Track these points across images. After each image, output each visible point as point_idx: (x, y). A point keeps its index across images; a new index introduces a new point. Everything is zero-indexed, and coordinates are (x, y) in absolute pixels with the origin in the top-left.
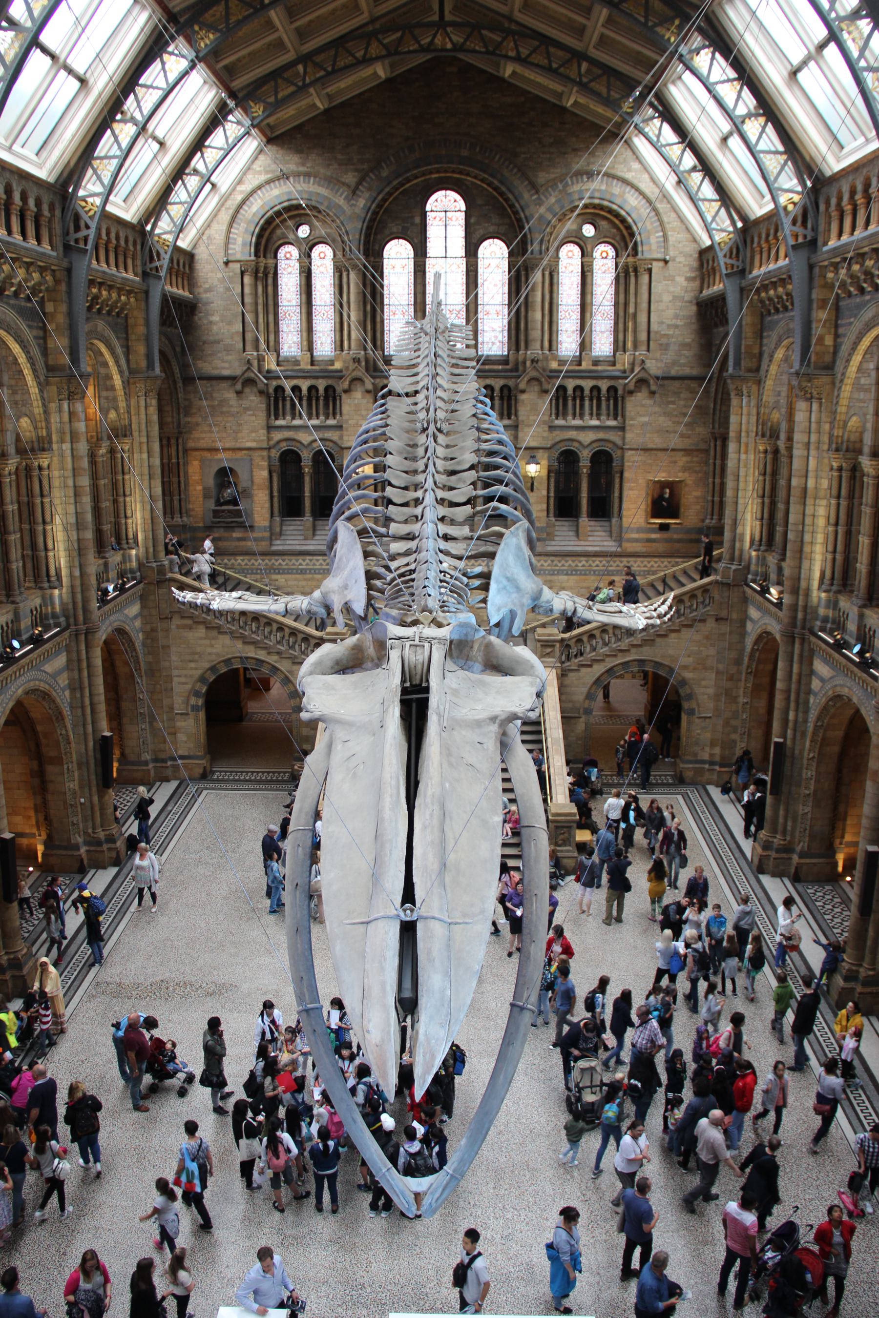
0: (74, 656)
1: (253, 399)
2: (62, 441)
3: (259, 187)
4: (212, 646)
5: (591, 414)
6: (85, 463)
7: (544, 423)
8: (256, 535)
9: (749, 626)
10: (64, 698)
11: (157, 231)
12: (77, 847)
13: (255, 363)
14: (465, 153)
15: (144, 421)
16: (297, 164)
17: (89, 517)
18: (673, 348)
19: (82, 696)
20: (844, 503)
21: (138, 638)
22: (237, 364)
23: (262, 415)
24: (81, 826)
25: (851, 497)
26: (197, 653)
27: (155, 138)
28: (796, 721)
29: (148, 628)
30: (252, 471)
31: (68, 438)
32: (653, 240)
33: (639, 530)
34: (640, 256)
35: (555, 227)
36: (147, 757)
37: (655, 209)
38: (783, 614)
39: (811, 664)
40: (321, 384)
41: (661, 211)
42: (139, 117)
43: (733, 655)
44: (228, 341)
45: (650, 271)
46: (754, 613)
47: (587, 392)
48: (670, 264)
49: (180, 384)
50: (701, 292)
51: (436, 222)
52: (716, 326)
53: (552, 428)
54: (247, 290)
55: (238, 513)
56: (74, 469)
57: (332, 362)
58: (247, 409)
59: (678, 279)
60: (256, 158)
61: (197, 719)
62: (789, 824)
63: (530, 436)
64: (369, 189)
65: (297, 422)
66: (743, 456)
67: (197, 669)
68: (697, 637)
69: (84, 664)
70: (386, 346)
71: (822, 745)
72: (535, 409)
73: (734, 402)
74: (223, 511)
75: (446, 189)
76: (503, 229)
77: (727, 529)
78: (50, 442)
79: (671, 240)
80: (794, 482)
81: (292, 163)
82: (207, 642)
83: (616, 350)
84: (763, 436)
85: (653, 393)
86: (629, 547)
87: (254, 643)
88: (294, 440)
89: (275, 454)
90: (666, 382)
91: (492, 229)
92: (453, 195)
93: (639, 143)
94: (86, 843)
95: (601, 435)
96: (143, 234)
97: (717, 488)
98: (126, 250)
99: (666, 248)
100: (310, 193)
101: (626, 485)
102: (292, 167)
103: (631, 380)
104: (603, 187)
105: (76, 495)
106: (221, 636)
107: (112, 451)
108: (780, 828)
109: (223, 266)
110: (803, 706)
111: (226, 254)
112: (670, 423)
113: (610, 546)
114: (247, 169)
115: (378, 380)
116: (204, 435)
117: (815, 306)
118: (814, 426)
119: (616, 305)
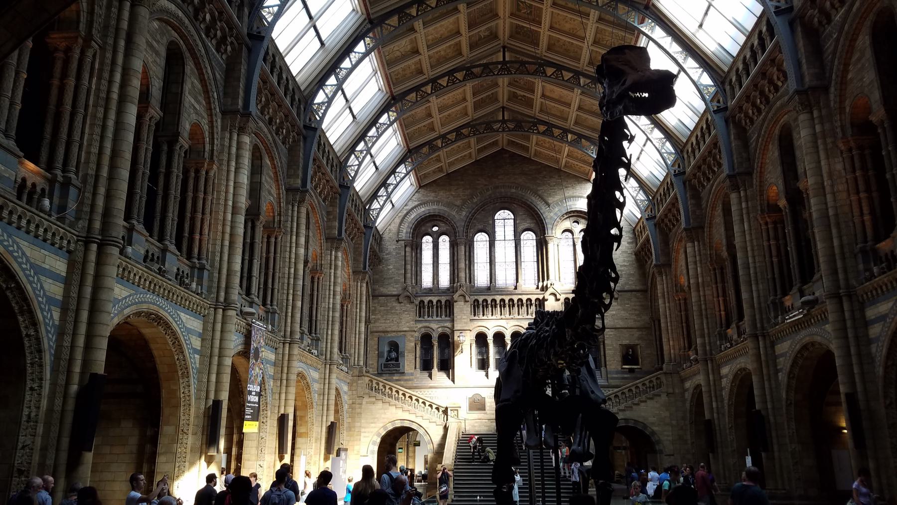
2: (330, 269)
3: (415, 207)
4: (385, 413)
8: (405, 378)
13: (410, 288)
14: (514, 191)
16: (433, 197)
20: (720, 285)
23: (413, 314)
28: (717, 407)
29: (351, 402)
31: (333, 267)
33: (617, 372)
40: (443, 299)
44: (397, 278)
49: (371, 298)
51: (500, 224)
54: (407, 254)
57: (448, 289)
58: (405, 311)
66: (667, 305)
69: (327, 381)
70: (476, 282)
73: (658, 279)
74: (389, 364)
76: (532, 226)
81: (431, 196)
82: (383, 411)
88: (428, 327)
89: (417, 334)
90: (622, 293)
91: (526, 225)
92: (507, 212)
101: (607, 348)
102: (432, 198)
106: (391, 408)
109: (396, 243)
110: (719, 398)
112: (628, 314)
115: (472, 297)
116: (381, 325)
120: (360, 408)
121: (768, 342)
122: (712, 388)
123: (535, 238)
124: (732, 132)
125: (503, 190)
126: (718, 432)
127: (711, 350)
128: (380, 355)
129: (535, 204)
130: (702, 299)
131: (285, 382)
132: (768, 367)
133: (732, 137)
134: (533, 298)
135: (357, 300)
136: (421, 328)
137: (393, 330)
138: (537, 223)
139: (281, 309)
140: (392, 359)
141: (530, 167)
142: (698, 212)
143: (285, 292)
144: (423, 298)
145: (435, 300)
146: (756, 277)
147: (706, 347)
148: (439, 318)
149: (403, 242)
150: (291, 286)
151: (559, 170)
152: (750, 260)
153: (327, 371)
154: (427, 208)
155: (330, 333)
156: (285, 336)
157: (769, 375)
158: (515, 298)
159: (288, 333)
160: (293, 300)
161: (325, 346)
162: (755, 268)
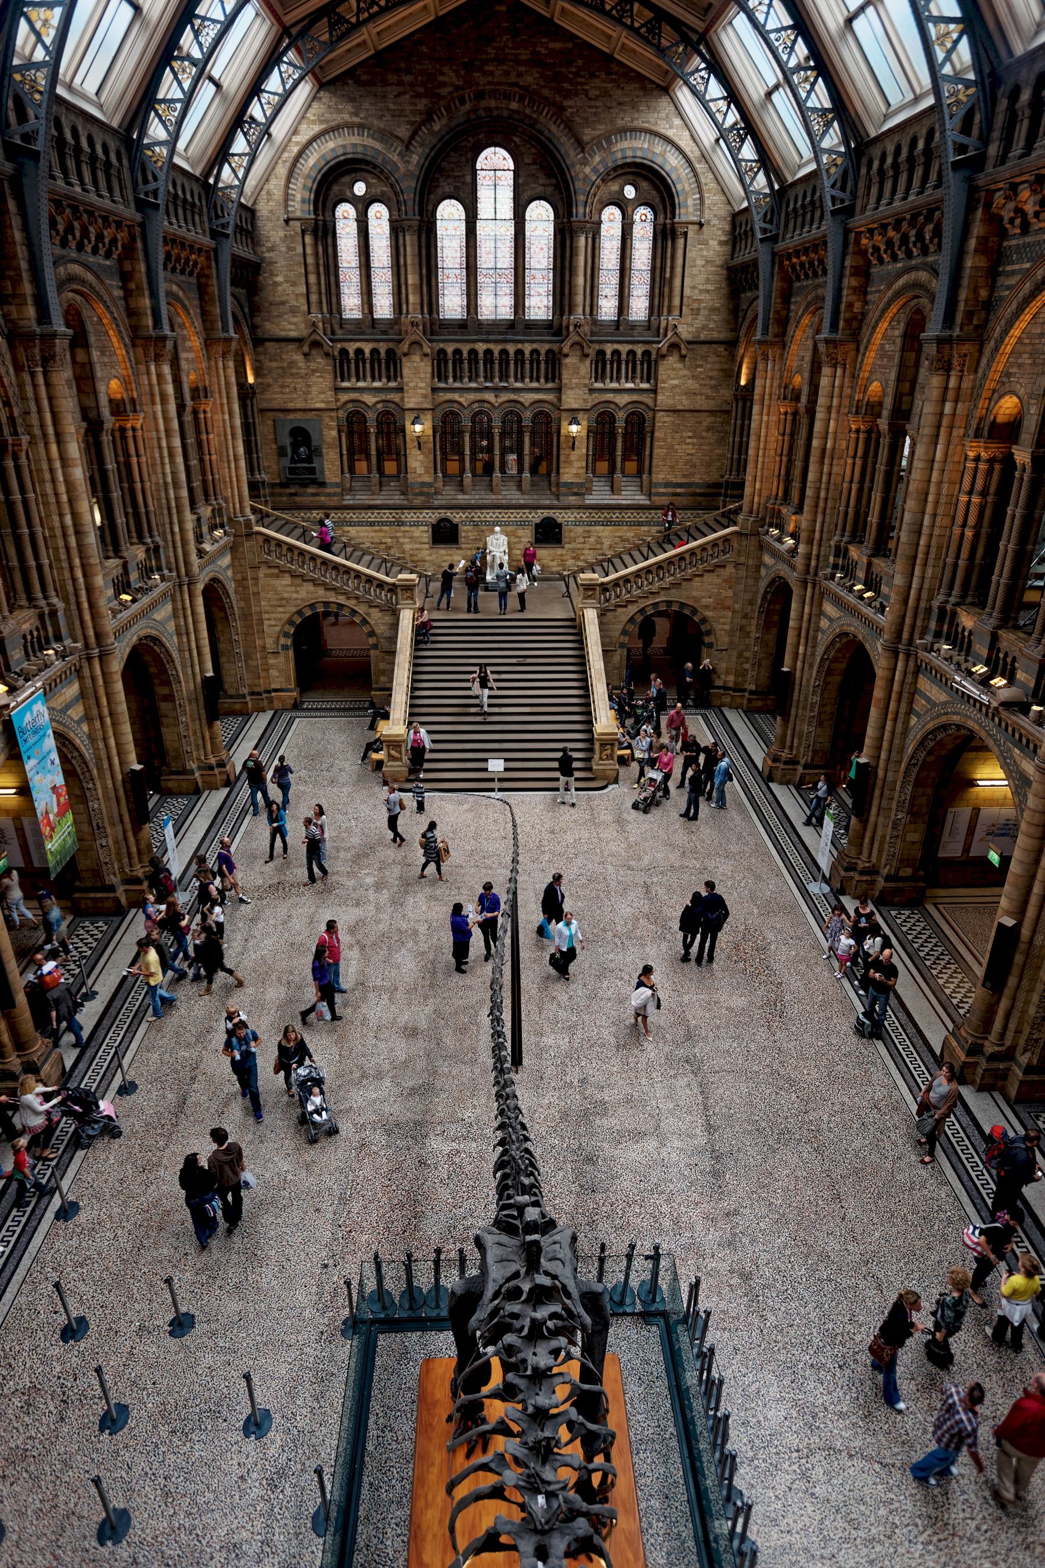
0: (180, 607)
1: (320, 362)
2: (153, 403)
4: (297, 592)
5: (627, 378)
6: (175, 425)
7: (585, 385)
8: (328, 490)
9: (763, 572)
10: (172, 643)
11: (220, 185)
12: (192, 772)
13: (320, 325)
14: (514, 105)
15: (223, 383)
16: (351, 114)
17: (183, 476)
18: (704, 312)
19: (189, 641)
20: (859, 462)
21: (231, 587)
22: (303, 326)
23: (329, 377)
24: (195, 754)
25: (865, 457)
26: (282, 599)
27: (211, 79)
28: (805, 654)
29: (239, 577)
30: (321, 431)
31: (158, 399)
32: (690, 202)
33: (667, 485)
34: (677, 220)
35: (598, 187)
36: (246, 691)
37: (693, 170)
38: (799, 561)
39: (821, 605)
40: (383, 348)
41: (699, 171)
42: (196, 54)
43: (748, 596)
44: (294, 303)
45: (686, 234)
46: (768, 559)
47: (624, 356)
48: (705, 228)
50: (732, 258)
52: (744, 291)
53: (592, 391)
54: (309, 250)
55: (312, 471)
56: (166, 431)
58: (314, 371)
59: (711, 242)
60: (310, 106)
61: (287, 658)
62: (796, 740)
63: (572, 399)
64: (422, 145)
65: (361, 384)
66: (765, 418)
67: (284, 614)
68: (719, 581)
69: (189, 612)
71: (827, 675)
72: (576, 371)
73: (760, 366)
75: (495, 145)
76: (549, 190)
77: (747, 484)
78: (141, 405)
79: (707, 202)
80: (815, 443)
82: (293, 589)
83: (651, 314)
84: (785, 398)
85: (683, 357)
86: (659, 501)
87: (335, 589)
89: (342, 414)
91: (539, 190)
92: (502, 152)
93: (684, 96)
94: (200, 768)
95: (635, 397)
96: (206, 186)
97: (736, 446)
98: (193, 205)
99: (702, 211)
100: (365, 146)
101: (656, 444)
102: (346, 117)
103: (663, 345)
104: (646, 146)
105: (171, 455)
107: (195, 412)
108: (788, 743)
110: (811, 641)
111: (287, 212)
113: (642, 499)
114: (302, 117)
117: (847, 272)
118: (836, 390)
119: (653, 270)
120: (257, 584)
121: (911, 664)
122: (804, 625)
123: (552, 217)
124: (977, 229)
125: (493, 104)
126: (797, 687)
127: (817, 567)
128: (281, 452)
129: (555, 141)
130: (825, 479)
131: (108, 721)
132: (899, 701)
133: (972, 243)
134: (543, 348)
135: (221, 397)
136: (347, 402)
137: (299, 406)
138: (557, 186)
139: (66, 599)
140: (302, 461)
141: (552, 45)
142: (857, 307)
143: (65, 564)
144: (346, 345)
145: (367, 348)
146: (927, 553)
147: (809, 559)
148: (377, 384)
149: (298, 224)
150: (75, 552)
151: (609, 58)
152: (927, 521)
153: (186, 597)
154: (340, 142)
155: (177, 529)
156: (87, 645)
157: (897, 713)
158: (511, 349)
159: (92, 640)
160: (85, 576)
161: (172, 554)
162: (931, 535)
